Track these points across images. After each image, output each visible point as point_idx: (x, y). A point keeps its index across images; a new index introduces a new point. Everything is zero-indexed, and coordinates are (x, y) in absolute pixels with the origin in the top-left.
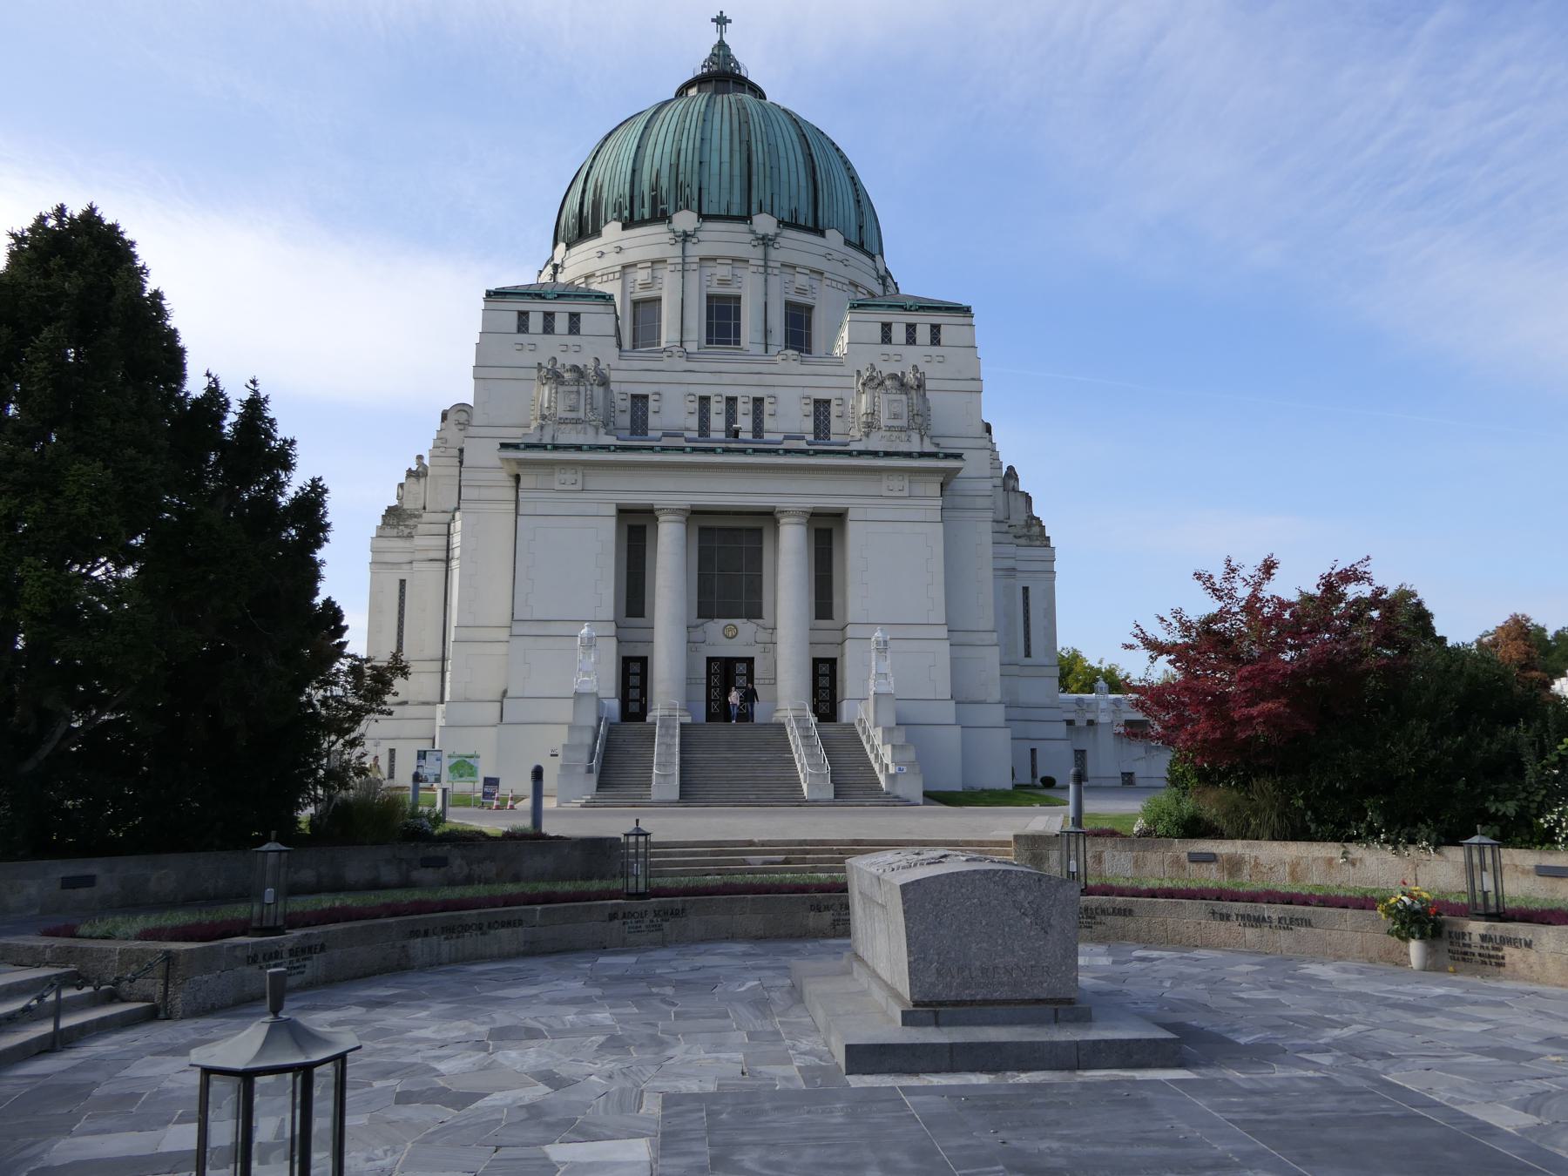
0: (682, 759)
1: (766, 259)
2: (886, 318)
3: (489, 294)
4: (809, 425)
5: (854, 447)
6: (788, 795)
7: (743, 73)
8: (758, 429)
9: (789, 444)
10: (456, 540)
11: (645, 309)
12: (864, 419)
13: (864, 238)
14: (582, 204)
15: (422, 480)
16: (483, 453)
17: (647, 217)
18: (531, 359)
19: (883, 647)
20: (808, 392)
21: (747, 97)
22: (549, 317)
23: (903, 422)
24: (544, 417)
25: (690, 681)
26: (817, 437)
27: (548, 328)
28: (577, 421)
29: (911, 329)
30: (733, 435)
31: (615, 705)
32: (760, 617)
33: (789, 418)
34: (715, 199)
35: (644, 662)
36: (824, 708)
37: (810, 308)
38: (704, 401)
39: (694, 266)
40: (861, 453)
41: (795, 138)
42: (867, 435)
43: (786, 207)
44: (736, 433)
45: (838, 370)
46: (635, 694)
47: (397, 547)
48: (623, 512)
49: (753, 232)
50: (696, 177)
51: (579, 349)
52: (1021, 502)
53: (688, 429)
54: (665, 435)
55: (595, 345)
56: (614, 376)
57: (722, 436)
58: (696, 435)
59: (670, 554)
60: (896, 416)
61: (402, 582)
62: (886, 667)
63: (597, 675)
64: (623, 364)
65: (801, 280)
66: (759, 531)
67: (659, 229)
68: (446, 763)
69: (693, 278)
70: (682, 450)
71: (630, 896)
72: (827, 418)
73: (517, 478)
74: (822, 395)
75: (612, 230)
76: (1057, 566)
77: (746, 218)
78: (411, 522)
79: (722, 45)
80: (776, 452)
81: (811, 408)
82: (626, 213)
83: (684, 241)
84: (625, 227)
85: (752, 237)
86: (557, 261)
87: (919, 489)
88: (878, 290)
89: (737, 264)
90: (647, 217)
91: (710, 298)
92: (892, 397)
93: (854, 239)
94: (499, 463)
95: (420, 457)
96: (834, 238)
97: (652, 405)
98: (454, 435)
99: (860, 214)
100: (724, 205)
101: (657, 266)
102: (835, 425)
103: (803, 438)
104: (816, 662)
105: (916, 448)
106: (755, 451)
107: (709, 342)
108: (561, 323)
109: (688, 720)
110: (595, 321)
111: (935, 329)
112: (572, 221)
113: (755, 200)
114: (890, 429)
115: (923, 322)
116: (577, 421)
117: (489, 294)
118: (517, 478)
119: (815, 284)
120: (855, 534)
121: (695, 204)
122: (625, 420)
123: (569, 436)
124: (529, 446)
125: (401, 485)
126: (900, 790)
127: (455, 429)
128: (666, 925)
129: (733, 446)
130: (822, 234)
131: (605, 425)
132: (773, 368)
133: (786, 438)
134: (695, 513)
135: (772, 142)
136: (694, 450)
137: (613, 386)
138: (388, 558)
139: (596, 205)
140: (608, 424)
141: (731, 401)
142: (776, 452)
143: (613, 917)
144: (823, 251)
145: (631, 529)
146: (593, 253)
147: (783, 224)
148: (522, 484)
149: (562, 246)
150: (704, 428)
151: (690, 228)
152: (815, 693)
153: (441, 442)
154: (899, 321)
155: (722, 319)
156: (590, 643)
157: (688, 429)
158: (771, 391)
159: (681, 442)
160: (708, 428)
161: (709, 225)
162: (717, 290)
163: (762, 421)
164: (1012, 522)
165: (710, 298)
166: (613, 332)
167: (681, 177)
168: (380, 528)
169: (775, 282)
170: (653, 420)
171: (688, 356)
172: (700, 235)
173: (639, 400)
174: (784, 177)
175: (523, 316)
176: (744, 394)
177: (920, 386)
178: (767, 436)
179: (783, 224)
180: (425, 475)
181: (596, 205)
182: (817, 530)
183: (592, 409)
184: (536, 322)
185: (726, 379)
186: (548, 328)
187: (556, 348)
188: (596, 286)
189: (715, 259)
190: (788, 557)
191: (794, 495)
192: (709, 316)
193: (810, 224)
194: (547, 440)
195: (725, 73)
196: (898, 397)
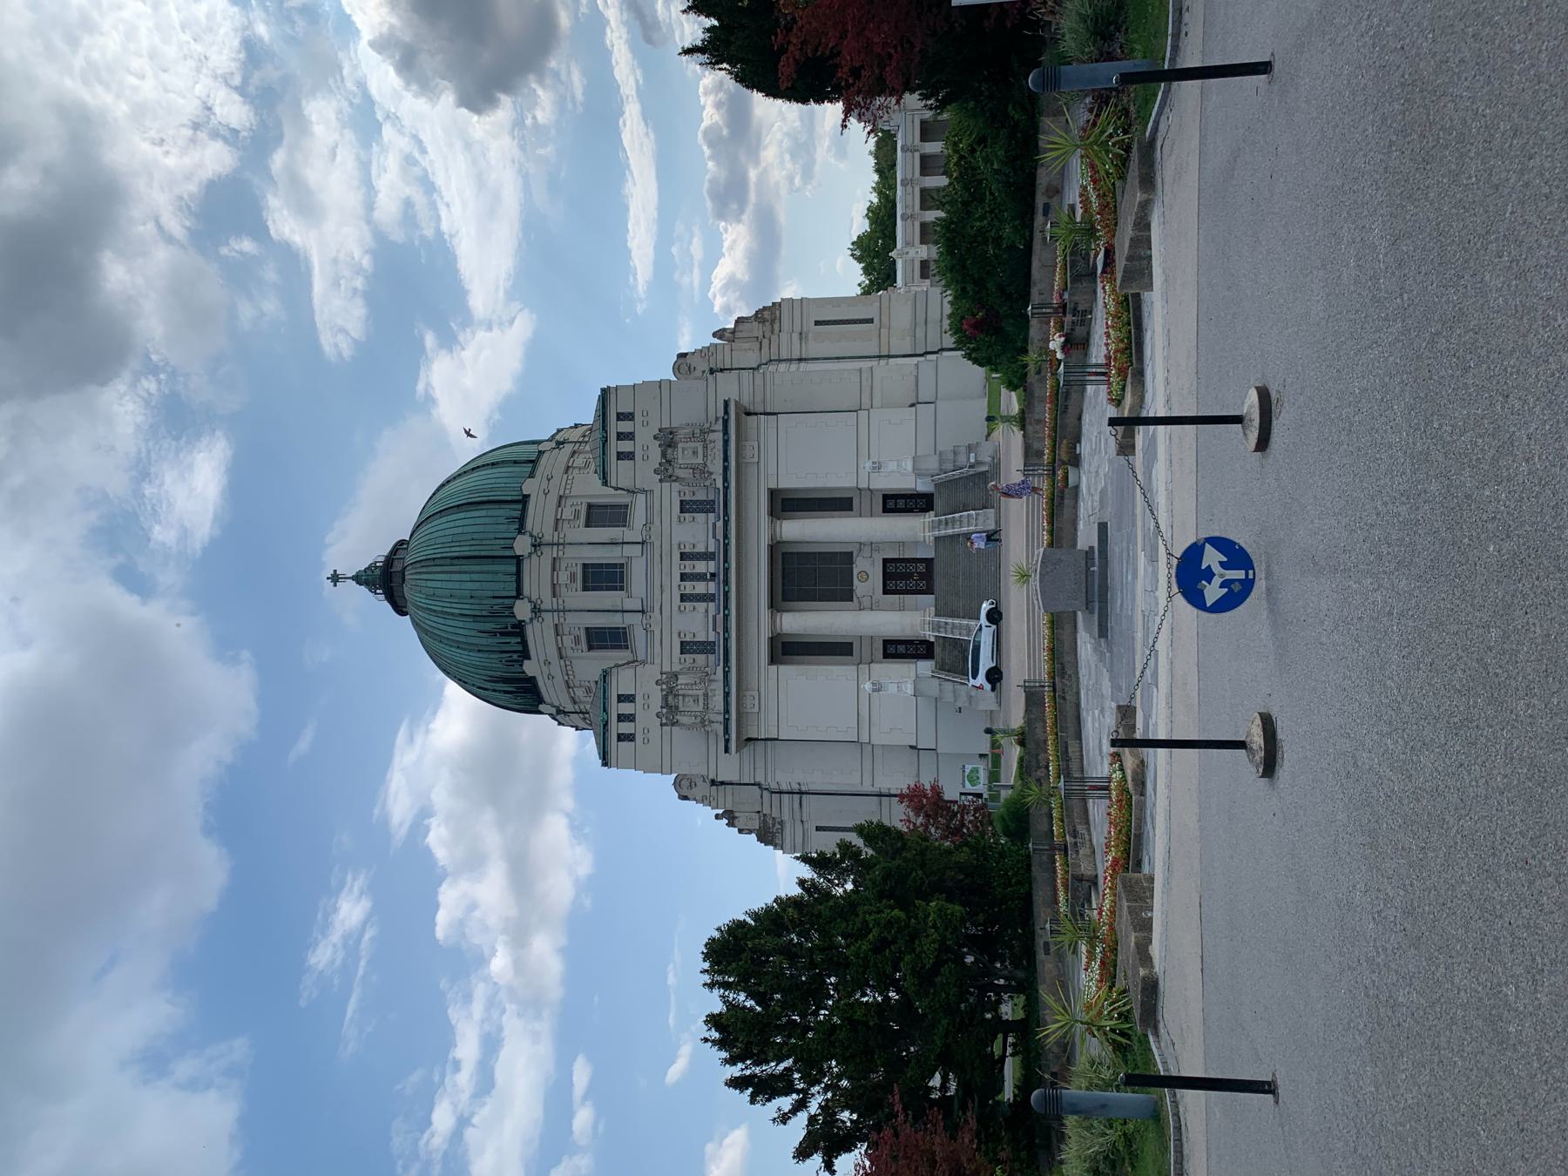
2: (614, 457)
3: (605, 764)
4: (701, 517)
5: (720, 484)
8: (707, 556)
9: (720, 536)
13: (522, 460)
16: (729, 768)
20: (675, 519)
22: (622, 718)
23: (700, 446)
24: (703, 721)
25: (902, 609)
27: (630, 718)
28: (706, 695)
29: (621, 436)
30: (713, 577)
33: (698, 532)
35: (887, 643)
36: (921, 503)
38: (684, 598)
40: (725, 479)
41: (444, 519)
44: (713, 575)
46: (911, 650)
48: (773, 660)
52: (741, 327)
56: (666, 668)
57: (712, 584)
60: (695, 453)
61: (818, 829)
63: (903, 677)
64: (657, 661)
70: (726, 617)
72: (695, 502)
77: (518, 560)
79: (358, 579)
82: (515, 656)
86: (553, 711)
88: (568, 448)
91: (585, 589)
93: (528, 468)
95: (717, 817)
96: (529, 487)
100: (508, 578)
104: (886, 510)
106: (726, 561)
108: (626, 708)
110: (623, 682)
111: (621, 417)
115: (615, 426)
116: (706, 695)
117: (605, 764)
118: (749, 739)
119: (569, 502)
121: (507, 601)
122: (701, 658)
123: (718, 702)
124: (726, 730)
125: (740, 831)
130: (528, 496)
134: (772, 605)
136: (726, 607)
137: (676, 668)
139: (505, 680)
142: (726, 546)
147: (521, 530)
149: (541, 707)
151: (529, 606)
153: (704, 800)
154: (615, 446)
155: (603, 577)
158: (675, 547)
161: (526, 591)
168: (775, 846)
170: (701, 637)
173: (686, 648)
174: (481, 528)
176: (678, 567)
178: (711, 549)
179: (521, 530)
181: (505, 680)
184: (626, 728)
186: (630, 718)
190: (801, 530)
191: (760, 530)
193: (520, 506)
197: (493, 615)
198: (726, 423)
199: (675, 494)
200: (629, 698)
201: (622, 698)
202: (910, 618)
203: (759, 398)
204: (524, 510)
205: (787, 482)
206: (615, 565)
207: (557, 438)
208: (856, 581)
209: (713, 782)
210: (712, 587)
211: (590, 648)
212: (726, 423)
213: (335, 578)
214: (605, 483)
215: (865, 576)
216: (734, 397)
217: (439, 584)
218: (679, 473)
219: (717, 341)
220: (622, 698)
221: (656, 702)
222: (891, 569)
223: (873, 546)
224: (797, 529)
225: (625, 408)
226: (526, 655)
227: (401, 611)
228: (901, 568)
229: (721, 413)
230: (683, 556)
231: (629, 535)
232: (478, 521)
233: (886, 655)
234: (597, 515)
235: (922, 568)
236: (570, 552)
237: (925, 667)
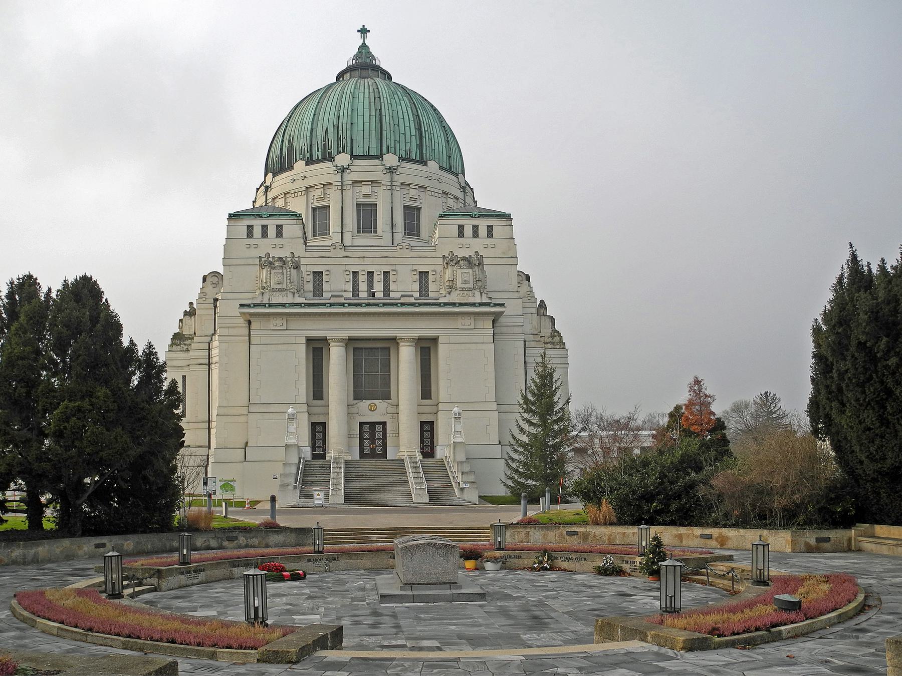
2: (461, 223)
3: (231, 217)
4: (416, 286)
5: (442, 300)
7: (378, 63)
9: (403, 300)
10: (215, 352)
11: (320, 212)
12: (447, 284)
14: (281, 149)
16: (229, 309)
18: (257, 253)
19: (458, 417)
20: (415, 267)
21: (380, 82)
22: (265, 228)
23: (470, 285)
24: (264, 288)
25: (350, 436)
27: (265, 235)
28: (282, 290)
29: (475, 228)
31: (307, 452)
33: (405, 285)
34: (361, 145)
35: (323, 425)
37: (419, 209)
38: (355, 274)
39: (349, 187)
40: (446, 304)
42: (449, 293)
45: (433, 254)
46: (319, 443)
48: (309, 340)
49: (384, 165)
50: (349, 133)
51: (282, 246)
53: (345, 291)
54: (332, 296)
55: (290, 245)
56: (302, 261)
57: (366, 295)
58: (350, 295)
60: (466, 282)
62: (459, 428)
64: (308, 255)
65: (414, 193)
66: (389, 348)
69: (348, 194)
70: (342, 305)
71: (316, 552)
73: (250, 323)
75: (300, 166)
77: (380, 157)
79: (364, 46)
80: (396, 304)
82: (308, 155)
83: (343, 172)
86: (268, 184)
87: (480, 324)
88: (460, 195)
89: (374, 185)
92: (464, 271)
96: (433, 165)
97: (325, 278)
98: (210, 290)
102: (432, 287)
103: (412, 296)
105: (477, 299)
108: (272, 231)
110: (291, 229)
111: (490, 228)
112: (275, 159)
113: (384, 145)
114: (463, 289)
115: (483, 224)
116: (282, 290)
118: (250, 323)
119: (422, 194)
120: (443, 349)
121: (349, 149)
122: (310, 287)
123: (278, 299)
124: (256, 305)
127: (211, 287)
131: (298, 291)
132: (395, 254)
134: (350, 341)
136: (349, 305)
137: (303, 268)
139: (290, 149)
140: (299, 291)
141: (371, 274)
142: (396, 304)
143: (309, 561)
144: (426, 175)
145: (315, 350)
146: (289, 179)
147: (401, 159)
148: (252, 327)
149: (270, 175)
151: (346, 164)
152: (422, 441)
153: (203, 293)
154: (468, 224)
155: (366, 218)
156: (293, 417)
157: (345, 291)
158: (394, 268)
159: (342, 301)
161: (357, 162)
163: (389, 285)
166: (300, 234)
167: (340, 133)
169: (397, 195)
170: (325, 287)
171: (345, 248)
172: (351, 168)
173: (318, 275)
175: (250, 228)
176: (378, 270)
177: (480, 264)
178: (392, 295)
181: (290, 149)
183: (291, 282)
184: (257, 231)
185: (367, 261)
186: (265, 235)
187: (268, 247)
189: (361, 182)
194: (265, 301)
196: (467, 271)
200: (279, 234)
201: (279, 228)
202: (341, 444)
203: (504, 330)
205: (442, 348)
206: (376, 226)
209: (216, 300)
210: (363, 294)
211: (314, 209)
213: (364, 31)
214: (441, 216)
215: (373, 409)
216: (507, 311)
217: (361, 100)
220: (279, 228)
222: (379, 428)
224: (407, 356)
227: (340, 76)
228: (379, 435)
229: (494, 301)
231: (399, 237)
233: (314, 425)
234: (412, 214)
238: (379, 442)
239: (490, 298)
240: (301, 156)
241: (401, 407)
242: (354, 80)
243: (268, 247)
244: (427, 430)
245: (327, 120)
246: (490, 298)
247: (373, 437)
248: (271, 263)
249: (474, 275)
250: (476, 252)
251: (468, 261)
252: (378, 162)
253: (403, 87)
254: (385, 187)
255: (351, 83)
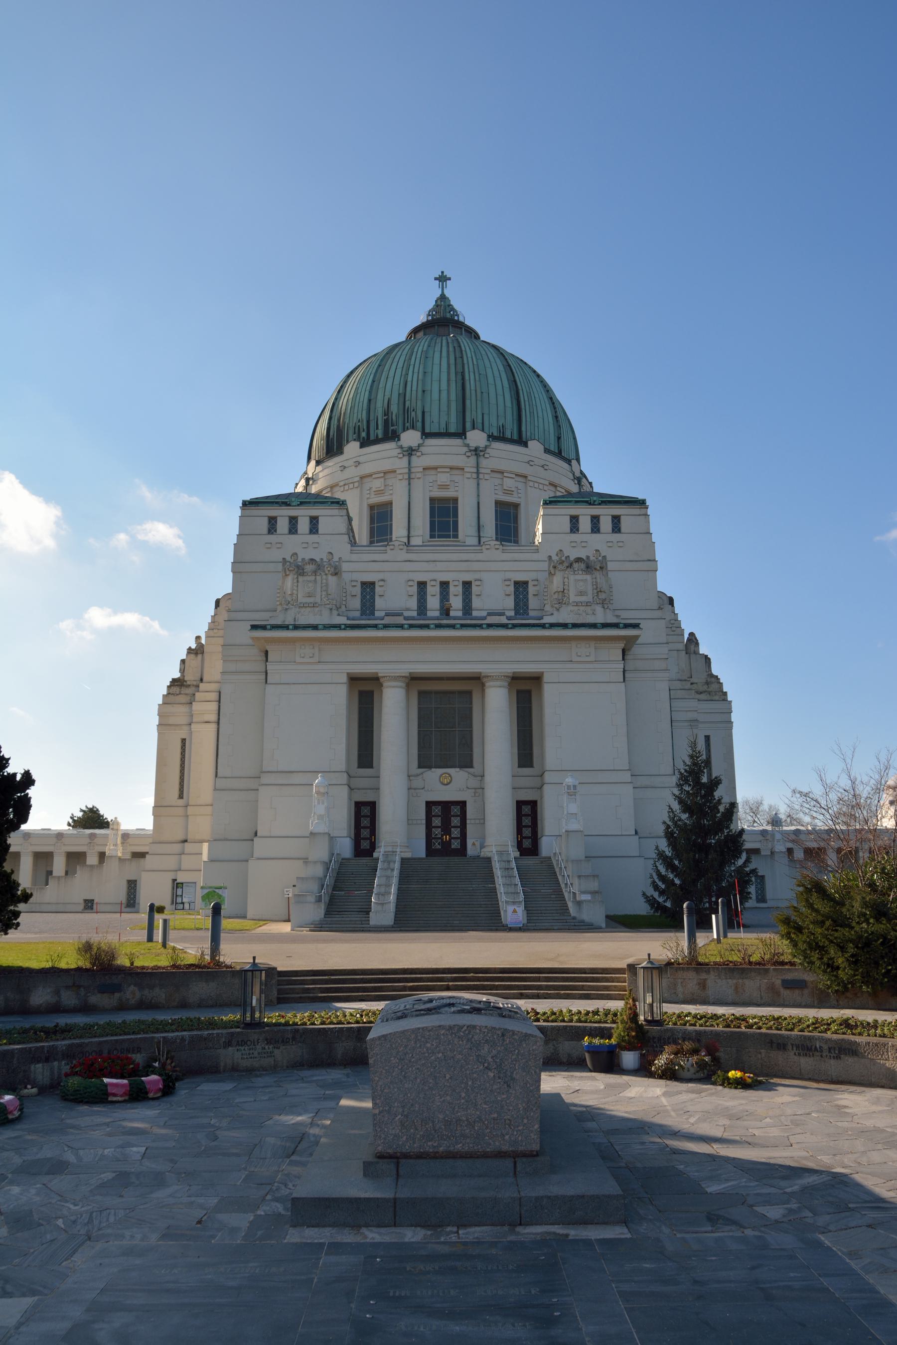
0: (400, 890)
1: (478, 467)
3: (246, 504)
4: (510, 603)
5: (547, 620)
6: (490, 921)
7: (461, 319)
8: (467, 608)
12: (556, 596)
13: (563, 447)
15: (200, 656)
17: (380, 436)
18: (277, 555)
19: (572, 792)
21: (464, 341)
22: (293, 521)
23: (588, 598)
25: (410, 821)
26: (363, 613)
28: (314, 605)
29: (595, 520)
30: (445, 612)
32: (472, 767)
33: (493, 597)
34: (436, 420)
35: (373, 805)
36: (527, 844)
37: (516, 506)
38: (422, 585)
39: (419, 475)
40: (552, 626)
41: (501, 368)
42: (558, 610)
43: (495, 424)
45: (535, 556)
46: (365, 833)
47: (179, 712)
48: (354, 680)
49: (468, 446)
53: (408, 609)
54: (387, 615)
55: (330, 541)
56: (345, 567)
57: (437, 614)
58: (415, 614)
59: (395, 715)
60: (582, 593)
62: (573, 808)
64: (354, 557)
65: (509, 483)
66: (470, 693)
67: (390, 446)
68: (199, 893)
69: (417, 485)
70: (401, 626)
74: (521, 577)
76: (734, 717)
77: (461, 434)
78: (190, 691)
79: (443, 297)
81: (512, 588)
82: (364, 434)
83: (410, 455)
84: (362, 446)
85: (466, 449)
90: (380, 436)
91: (432, 500)
93: (553, 447)
94: (250, 642)
96: (535, 447)
97: (378, 590)
99: (558, 427)
100: (443, 425)
101: (388, 476)
102: (533, 603)
104: (520, 804)
105: (600, 619)
106: (463, 626)
107: (432, 536)
108: (303, 525)
109: (408, 855)
110: (330, 520)
111: (616, 520)
113: (468, 419)
114: (577, 604)
115: (606, 513)
116: (314, 605)
118: (266, 653)
119: (521, 486)
121: (419, 424)
122: (356, 603)
125: (183, 661)
126: (586, 915)
128: (276, 1051)
129: (445, 622)
130: (525, 445)
133: (387, 615)
134: (413, 680)
135: (482, 372)
136: (411, 626)
137: (346, 577)
138: (172, 720)
141: (444, 585)
142: (480, 626)
144: (527, 459)
145: (361, 694)
147: (492, 437)
150: (422, 607)
153: (214, 625)
154: (585, 513)
155: (443, 518)
157: (408, 609)
159: (400, 620)
160: (425, 608)
162: (438, 494)
164: (693, 680)
165: (432, 500)
166: (343, 528)
167: (408, 404)
170: (379, 603)
172: (422, 449)
173: (368, 588)
175: (272, 521)
176: (456, 579)
178: (475, 613)
179: (492, 437)
180: (203, 653)
182: (518, 692)
183: (328, 594)
184: (283, 525)
187: (300, 546)
188: (339, 495)
189: (435, 468)
190: (495, 715)
191: (496, 661)
192: (432, 515)
193: (515, 437)
194: (289, 621)
195: (445, 318)
197: (406, 411)
198: (615, 626)
199: (533, 576)
202: (400, 832)
204: (511, 441)
206: (456, 529)
207: (584, 480)
208: (440, 771)
212: (615, 626)
213: (443, 279)
218: (557, 581)
219: (686, 636)
221: (305, 554)
222: (456, 810)
223: (480, 790)
225: (625, 524)
226: (365, 443)
228: (456, 821)
230: (467, 585)
232: (501, 399)
233: (358, 805)
235: (455, 845)
236: (471, 485)
237: (346, 847)
238: (456, 833)
239: (618, 616)
240: (355, 436)
241: (487, 778)
242: (428, 338)
243: (300, 546)
244: (527, 815)
245: (389, 388)
246: (618, 616)
247: (446, 823)
248: (298, 567)
249: (596, 586)
250: (597, 551)
251: (588, 566)
252: (458, 441)
253: (495, 347)
254: (468, 475)
255: (424, 341)
